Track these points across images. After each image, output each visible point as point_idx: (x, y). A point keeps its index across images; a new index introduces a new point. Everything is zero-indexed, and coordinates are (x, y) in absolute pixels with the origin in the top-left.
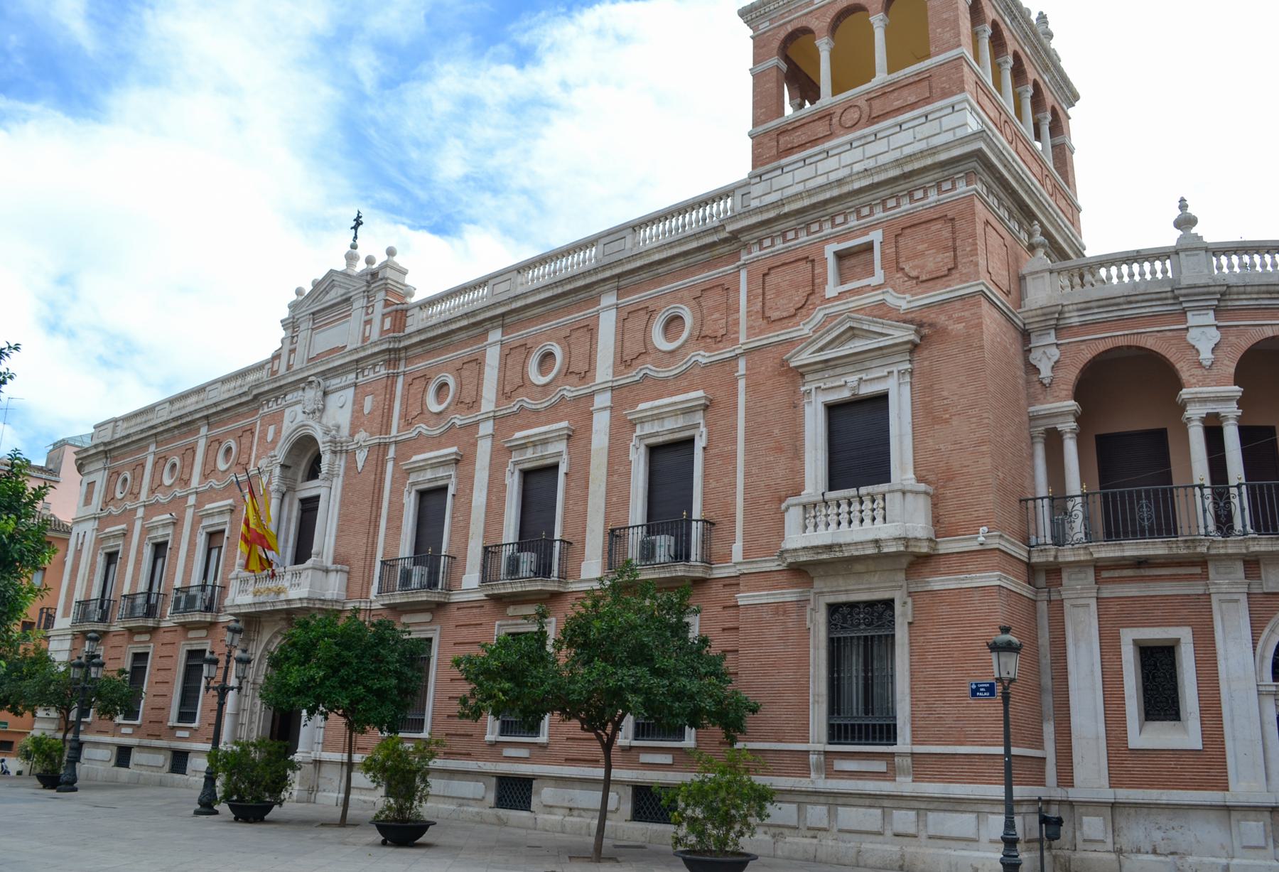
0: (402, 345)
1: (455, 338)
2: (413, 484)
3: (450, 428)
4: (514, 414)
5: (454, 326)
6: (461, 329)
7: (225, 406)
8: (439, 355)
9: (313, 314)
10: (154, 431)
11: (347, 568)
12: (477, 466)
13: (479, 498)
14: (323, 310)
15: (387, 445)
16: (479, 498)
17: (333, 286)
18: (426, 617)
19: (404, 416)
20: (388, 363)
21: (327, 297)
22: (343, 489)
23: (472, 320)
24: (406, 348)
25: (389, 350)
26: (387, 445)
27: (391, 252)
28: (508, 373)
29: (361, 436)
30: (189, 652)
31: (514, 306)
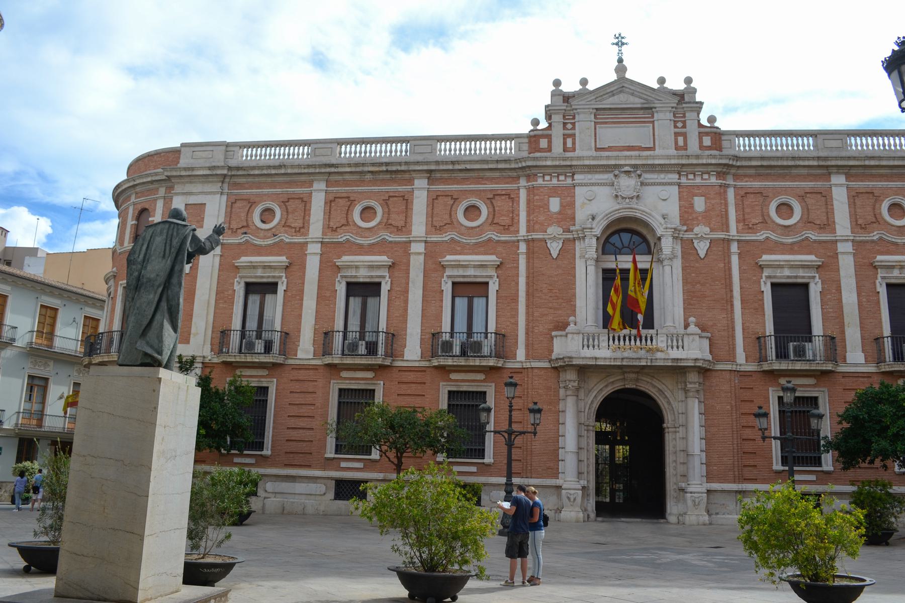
0: (739, 164)
1: (794, 171)
2: (768, 277)
3: (803, 240)
4: (873, 241)
5: (801, 163)
6: (804, 166)
7: (468, 167)
8: (774, 181)
9: (597, 109)
10: (328, 170)
11: (709, 335)
12: (842, 273)
13: (850, 297)
14: (610, 109)
15: (728, 241)
16: (850, 297)
17: (621, 92)
18: (811, 381)
19: (742, 220)
20: (720, 175)
21: (611, 100)
22: (684, 269)
23: (821, 163)
24: (739, 167)
25: (725, 165)
26: (728, 241)
27: (688, 80)
28: (858, 210)
29: (701, 229)
30: (450, 392)
31: (867, 163)
